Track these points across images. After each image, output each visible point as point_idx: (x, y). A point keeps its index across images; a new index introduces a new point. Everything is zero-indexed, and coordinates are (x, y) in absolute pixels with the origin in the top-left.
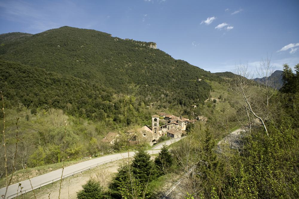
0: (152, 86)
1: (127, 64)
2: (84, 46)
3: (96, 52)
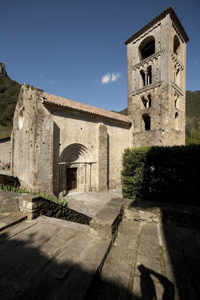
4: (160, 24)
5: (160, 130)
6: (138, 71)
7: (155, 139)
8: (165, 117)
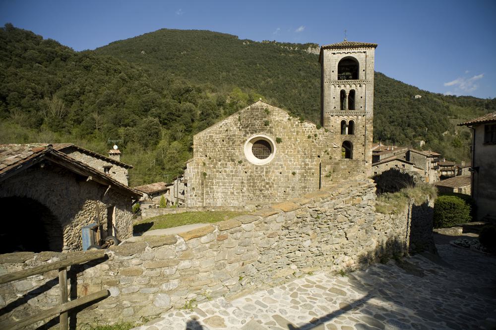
0: (312, 114)
1: (264, 80)
2: (187, 51)
3: (209, 62)
4: (364, 52)
5: (364, 161)
6: (338, 90)
7: (358, 170)
8: (369, 149)
